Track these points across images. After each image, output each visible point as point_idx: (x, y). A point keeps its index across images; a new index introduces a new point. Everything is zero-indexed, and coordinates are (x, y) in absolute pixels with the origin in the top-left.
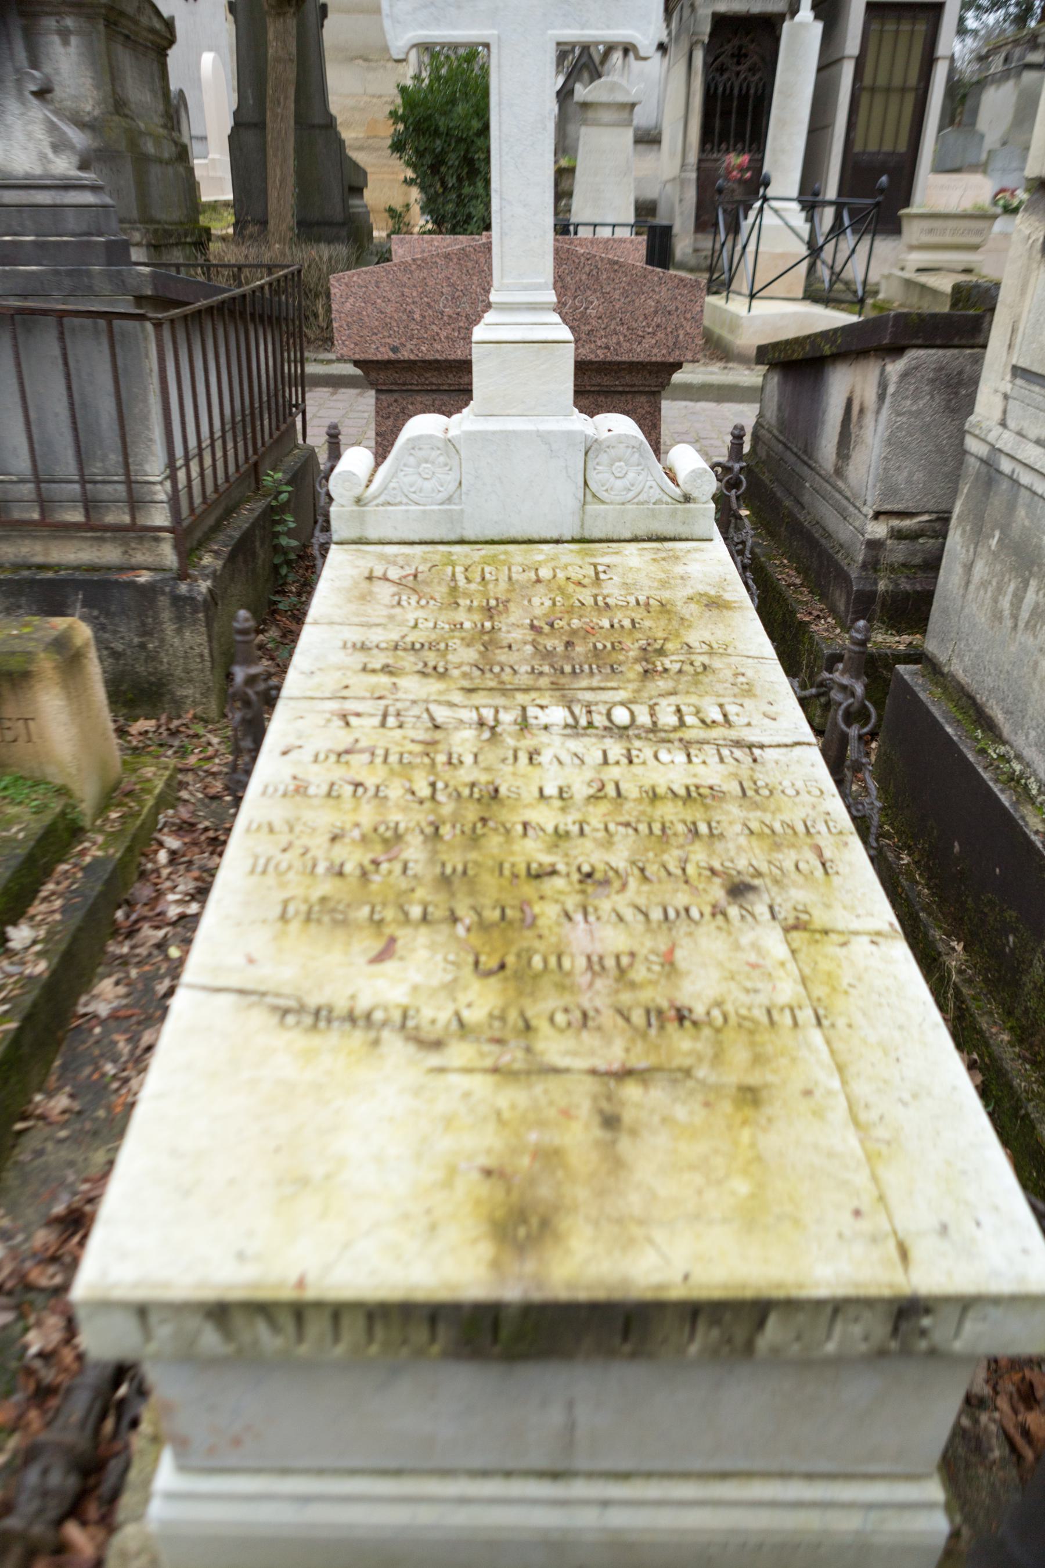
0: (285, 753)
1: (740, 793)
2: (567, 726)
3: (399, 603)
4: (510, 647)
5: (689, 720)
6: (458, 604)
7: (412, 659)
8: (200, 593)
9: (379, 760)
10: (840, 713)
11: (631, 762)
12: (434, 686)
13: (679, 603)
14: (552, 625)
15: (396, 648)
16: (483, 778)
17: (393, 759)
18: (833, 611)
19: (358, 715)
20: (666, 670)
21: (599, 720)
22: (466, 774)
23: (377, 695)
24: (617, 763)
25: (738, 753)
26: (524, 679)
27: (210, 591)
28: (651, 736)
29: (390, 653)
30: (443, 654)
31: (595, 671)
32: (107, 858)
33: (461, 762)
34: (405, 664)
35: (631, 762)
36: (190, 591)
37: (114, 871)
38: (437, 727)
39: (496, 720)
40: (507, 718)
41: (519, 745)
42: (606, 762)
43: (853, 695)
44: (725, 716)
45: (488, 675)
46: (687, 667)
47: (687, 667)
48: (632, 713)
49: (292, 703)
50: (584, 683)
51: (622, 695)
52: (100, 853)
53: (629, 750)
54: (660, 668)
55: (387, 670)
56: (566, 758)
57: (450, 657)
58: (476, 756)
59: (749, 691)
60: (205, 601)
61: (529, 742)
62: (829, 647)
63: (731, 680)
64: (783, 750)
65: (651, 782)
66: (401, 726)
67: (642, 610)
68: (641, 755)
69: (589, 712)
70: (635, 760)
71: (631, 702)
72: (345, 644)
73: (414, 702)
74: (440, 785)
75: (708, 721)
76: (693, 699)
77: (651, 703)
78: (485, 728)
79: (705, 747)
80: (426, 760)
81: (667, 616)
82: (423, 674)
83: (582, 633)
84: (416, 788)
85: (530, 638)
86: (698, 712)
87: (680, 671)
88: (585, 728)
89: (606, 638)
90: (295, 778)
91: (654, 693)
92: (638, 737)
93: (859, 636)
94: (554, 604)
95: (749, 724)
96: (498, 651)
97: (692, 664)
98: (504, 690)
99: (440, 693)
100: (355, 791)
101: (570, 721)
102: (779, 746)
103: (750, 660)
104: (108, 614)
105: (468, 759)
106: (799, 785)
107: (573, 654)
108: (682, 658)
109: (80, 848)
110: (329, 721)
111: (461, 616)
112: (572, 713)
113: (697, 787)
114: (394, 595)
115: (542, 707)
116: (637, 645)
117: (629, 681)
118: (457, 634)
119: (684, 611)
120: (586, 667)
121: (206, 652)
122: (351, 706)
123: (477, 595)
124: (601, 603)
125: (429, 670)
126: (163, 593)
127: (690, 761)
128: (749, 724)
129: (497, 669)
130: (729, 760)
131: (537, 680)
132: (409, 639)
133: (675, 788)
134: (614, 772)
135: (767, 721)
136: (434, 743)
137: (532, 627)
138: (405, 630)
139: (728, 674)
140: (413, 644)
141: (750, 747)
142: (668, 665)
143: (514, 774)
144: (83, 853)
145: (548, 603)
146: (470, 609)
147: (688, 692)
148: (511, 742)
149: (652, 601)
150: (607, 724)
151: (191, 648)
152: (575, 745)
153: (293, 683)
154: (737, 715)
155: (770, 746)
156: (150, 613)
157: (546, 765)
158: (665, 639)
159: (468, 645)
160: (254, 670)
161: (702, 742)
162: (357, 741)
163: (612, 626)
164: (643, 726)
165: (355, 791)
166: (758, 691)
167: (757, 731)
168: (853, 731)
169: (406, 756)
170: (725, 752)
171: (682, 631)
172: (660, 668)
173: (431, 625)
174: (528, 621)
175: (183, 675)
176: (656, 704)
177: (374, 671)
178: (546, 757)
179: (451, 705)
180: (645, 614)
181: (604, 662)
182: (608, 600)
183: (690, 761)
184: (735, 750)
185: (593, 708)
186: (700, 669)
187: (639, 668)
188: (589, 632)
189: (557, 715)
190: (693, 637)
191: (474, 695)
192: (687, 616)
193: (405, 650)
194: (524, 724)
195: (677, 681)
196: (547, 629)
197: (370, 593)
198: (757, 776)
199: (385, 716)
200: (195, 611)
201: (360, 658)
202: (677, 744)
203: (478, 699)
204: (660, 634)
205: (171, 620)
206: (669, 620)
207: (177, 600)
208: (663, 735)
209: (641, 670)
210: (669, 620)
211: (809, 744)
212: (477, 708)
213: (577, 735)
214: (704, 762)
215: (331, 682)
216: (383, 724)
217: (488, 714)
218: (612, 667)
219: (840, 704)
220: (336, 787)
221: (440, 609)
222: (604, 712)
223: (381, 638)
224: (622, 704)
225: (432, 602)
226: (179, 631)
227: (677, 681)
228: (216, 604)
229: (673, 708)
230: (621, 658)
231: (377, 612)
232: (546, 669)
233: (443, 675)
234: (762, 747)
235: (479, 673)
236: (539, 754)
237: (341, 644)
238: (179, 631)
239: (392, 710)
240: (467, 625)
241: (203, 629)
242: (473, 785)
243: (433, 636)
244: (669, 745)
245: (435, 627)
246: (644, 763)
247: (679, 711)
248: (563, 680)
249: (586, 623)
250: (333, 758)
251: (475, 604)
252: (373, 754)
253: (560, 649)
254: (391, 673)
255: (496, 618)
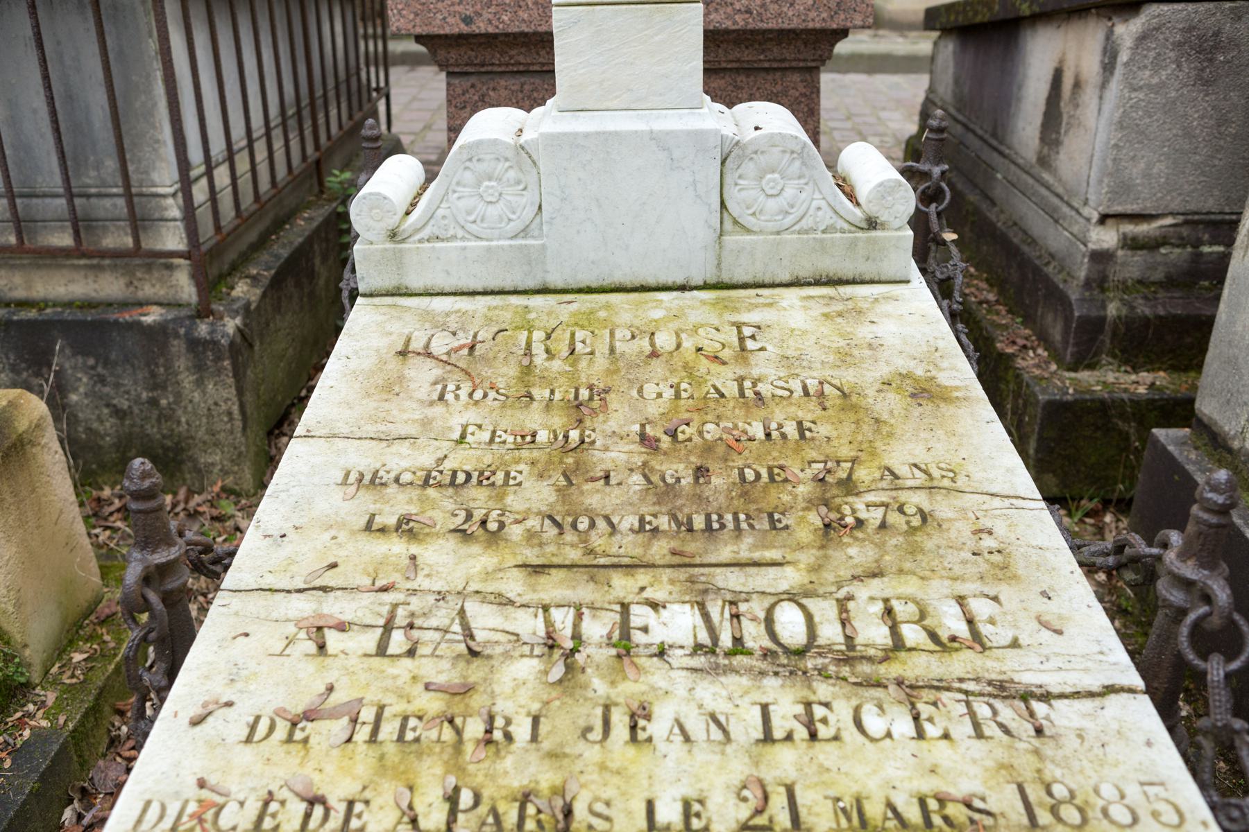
0: (196, 722)
1: (1025, 820)
2: (698, 648)
3: (441, 398)
4: (607, 477)
5: (912, 634)
6: (532, 398)
7: (449, 505)
8: (224, 335)
9: (363, 733)
10: (1184, 630)
11: (813, 736)
12: (478, 560)
13: (871, 392)
14: (673, 434)
15: (426, 483)
16: (546, 778)
17: (389, 730)
18: (1044, 339)
19: (342, 627)
20: (860, 523)
21: (754, 636)
22: (518, 769)
23: (379, 584)
24: (789, 737)
25: (1007, 713)
26: (628, 545)
27: (239, 329)
28: (845, 671)
29: (415, 493)
30: (499, 492)
31: (744, 526)
32: (54, 730)
33: (508, 737)
34: (437, 515)
35: (813, 736)
36: (212, 332)
37: (63, 749)
38: (473, 653)
39: (577, 636)
40: (596, 629)
41: (613, 693)
42: (768, 737)
43: (1207, 598)
44: (970, 622)
45: (570, 537)
46: (894, 518)
47: (894, 518)
48: (809, 618)
49: (236, 602)
50: (726, 552)
51: (789, 578)
52: (44, 723)
53: (808, 705)
54: (849, 520)
55: (406, 528)
56: (696, 726)
57: (509, 500)
58: (536, 720)
59: (1005, 567)
60: (232, 344)
61: (629, 690)
62: (1044, 391)
63: (971, 544)
64: (1087, 705)
65: (855, 788)
66: (411, 653)
67: (813, 404)
68: (832, 718)
69: (736, 616)
70: (823, 731)
71: (807, 595)
72: (347, 475)
73: (441, 596)
74: (466, 798)
75: (944, 636)
76: (910, 586)
77: (842, 594)
78: (557, 653)
79: (945, 696)
80: (448, 734)
81: (853, 417)
82: (461, 533)
83: (721, 450)
84: (420, 808)
85: (638, 460)
86: (923, 615)
87: (883, 526)
88: (728, 654)
89: (759, 458)
90: (202, 784)
91: (845, 573)
92: (822, 672)
93: (1220, 499)
94: (678, 396)
95: (1015, 644)
96: (588, 487)
97: (901, 510)
98: (594, 569)
99: (487, 575)
100: (308, 816)
101: (704, 637)
102: (1076, 695)
103: (997, 502)
104: (106, 364)
105: (522, 730)
106: (1133, 792)
107: (708, 492)
108: (884, 497)
109: (19, 715)
110: (290, 641)
111: (534, 419)
112: (706, 616)
113: (942, 801)
114: (435, 383)
115: (655, 606)
116: (809, 473)
117: (801, 547)
118: (525, 454)
119: (878, 407)
120: (729, 517)
121: (236, 409)
122: (336, 607)
123: (562, 380)
124: (749, 393)
125: (473, 527)
126: (177, 336)
127: (920, 735)
128: (1015, 644)
129: (583, 524)
130: (990, 729)
131: (647, 546)
132: (447, 465)
133: (900, 801)
134: (784, 762)
135: (1046, 635)
136: (466, 690)
137: (643, 438)
138: (446, 446)
139: (961, 530)
140: (454, 473)
141: (1026, 697)
142: (863, 515)
143: (603, 767)
144: (20, 724)
145: (668, 393)
146: (549, 405)
147: (901, 571)
148: (599, 686)
149: (828, 389)
150: (768, 643)
151: (216, 404)
152: (713, 694)
153: (252, 558)
154: (992, 621)
155: (1062, 696)
156: (161, 361)
157: (661, 746)
158: (854, 461)
159: (541, 476)
160: (160, 557)
161: (940, 686)
162: (330, 689)
163: (768, 435)
164: (829, 648)
165: (308, 816)
166: (1019, 567)
167: (1032, 660)
168: (1216, 669)
169: (412, 722)
170: (983, 711)
171: (878, 444)
172: (849, 520)
173: (486, 436)
174: (637, 428)
175: (206, 437)
176: (850, 598)
177: (382, 530)
178: (658, 727)
179: (503, 602)
180: (819, 412)
181: (757, 508)
182: (761, 387)
183: (920, 735)
184: (998, 704)
185: (743, 607)
186: (916, 521)
187: (815, 519)
188: (735, 444)
189: (679, 624)
190: (899, 456)
191: (543, 579)
192: (885, 417)
193: (440, 485)
194: (623, 645)
195: (881, 546)
196: (666, 442)
197: (401, 378)
198: (1052, 771)
199: (388, 628)
200: (218, 359)
201: (366, 502)
202: (892, 688)
203: (553, 588)
204: (846, 452)
205: (188, 369)
206: (857, 422)
207: (195, 345)
208: (865, 668)
209: (819, 524)
210: (857, 422)
211: (1131, 691)
212: (546, 608)
213: (716, 671)
214: (946, 736)
215: (306, 556)
216: (382, 650)
217: (563, 620)
218: (771, 515)
219: (1183, 612)
220: (274, 807)
221: (503, 406)
222: (762, 615)
223: (405, 464)
224: (792, 597)
225: (492, 394)
226: (200, 383)
227: (881, 546)
228: (251, 346)
229: (878, 607)
230: (786, 498)
231: (405, 415)
232: (664, 522)
233: (494, 537)
234: (1046, 697)
235: (555, 531)
236: (648, 717)
237: (339, 477)
238: (200, 383)
239: (401, 617)
240: (543, 436)
241: (231, 381)
242: (525, 798)
243: (488, 459)
244: (878, 693)
245: (492, 441)
246: (836, 738)
247: (889, 612)
248: (691, 547)
249: (725, 429)
250: (282, 729)
251: (558, 396)
252: (354, 721)
253: (687, 481)
254: (412, 535)
255: (588, 423)
